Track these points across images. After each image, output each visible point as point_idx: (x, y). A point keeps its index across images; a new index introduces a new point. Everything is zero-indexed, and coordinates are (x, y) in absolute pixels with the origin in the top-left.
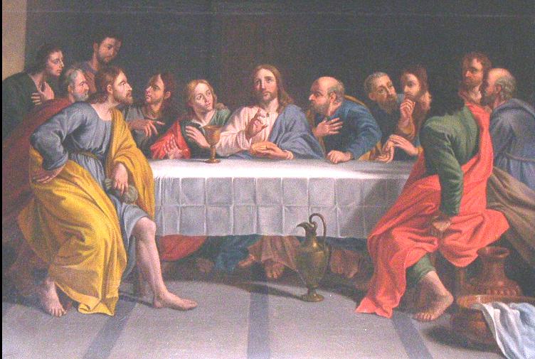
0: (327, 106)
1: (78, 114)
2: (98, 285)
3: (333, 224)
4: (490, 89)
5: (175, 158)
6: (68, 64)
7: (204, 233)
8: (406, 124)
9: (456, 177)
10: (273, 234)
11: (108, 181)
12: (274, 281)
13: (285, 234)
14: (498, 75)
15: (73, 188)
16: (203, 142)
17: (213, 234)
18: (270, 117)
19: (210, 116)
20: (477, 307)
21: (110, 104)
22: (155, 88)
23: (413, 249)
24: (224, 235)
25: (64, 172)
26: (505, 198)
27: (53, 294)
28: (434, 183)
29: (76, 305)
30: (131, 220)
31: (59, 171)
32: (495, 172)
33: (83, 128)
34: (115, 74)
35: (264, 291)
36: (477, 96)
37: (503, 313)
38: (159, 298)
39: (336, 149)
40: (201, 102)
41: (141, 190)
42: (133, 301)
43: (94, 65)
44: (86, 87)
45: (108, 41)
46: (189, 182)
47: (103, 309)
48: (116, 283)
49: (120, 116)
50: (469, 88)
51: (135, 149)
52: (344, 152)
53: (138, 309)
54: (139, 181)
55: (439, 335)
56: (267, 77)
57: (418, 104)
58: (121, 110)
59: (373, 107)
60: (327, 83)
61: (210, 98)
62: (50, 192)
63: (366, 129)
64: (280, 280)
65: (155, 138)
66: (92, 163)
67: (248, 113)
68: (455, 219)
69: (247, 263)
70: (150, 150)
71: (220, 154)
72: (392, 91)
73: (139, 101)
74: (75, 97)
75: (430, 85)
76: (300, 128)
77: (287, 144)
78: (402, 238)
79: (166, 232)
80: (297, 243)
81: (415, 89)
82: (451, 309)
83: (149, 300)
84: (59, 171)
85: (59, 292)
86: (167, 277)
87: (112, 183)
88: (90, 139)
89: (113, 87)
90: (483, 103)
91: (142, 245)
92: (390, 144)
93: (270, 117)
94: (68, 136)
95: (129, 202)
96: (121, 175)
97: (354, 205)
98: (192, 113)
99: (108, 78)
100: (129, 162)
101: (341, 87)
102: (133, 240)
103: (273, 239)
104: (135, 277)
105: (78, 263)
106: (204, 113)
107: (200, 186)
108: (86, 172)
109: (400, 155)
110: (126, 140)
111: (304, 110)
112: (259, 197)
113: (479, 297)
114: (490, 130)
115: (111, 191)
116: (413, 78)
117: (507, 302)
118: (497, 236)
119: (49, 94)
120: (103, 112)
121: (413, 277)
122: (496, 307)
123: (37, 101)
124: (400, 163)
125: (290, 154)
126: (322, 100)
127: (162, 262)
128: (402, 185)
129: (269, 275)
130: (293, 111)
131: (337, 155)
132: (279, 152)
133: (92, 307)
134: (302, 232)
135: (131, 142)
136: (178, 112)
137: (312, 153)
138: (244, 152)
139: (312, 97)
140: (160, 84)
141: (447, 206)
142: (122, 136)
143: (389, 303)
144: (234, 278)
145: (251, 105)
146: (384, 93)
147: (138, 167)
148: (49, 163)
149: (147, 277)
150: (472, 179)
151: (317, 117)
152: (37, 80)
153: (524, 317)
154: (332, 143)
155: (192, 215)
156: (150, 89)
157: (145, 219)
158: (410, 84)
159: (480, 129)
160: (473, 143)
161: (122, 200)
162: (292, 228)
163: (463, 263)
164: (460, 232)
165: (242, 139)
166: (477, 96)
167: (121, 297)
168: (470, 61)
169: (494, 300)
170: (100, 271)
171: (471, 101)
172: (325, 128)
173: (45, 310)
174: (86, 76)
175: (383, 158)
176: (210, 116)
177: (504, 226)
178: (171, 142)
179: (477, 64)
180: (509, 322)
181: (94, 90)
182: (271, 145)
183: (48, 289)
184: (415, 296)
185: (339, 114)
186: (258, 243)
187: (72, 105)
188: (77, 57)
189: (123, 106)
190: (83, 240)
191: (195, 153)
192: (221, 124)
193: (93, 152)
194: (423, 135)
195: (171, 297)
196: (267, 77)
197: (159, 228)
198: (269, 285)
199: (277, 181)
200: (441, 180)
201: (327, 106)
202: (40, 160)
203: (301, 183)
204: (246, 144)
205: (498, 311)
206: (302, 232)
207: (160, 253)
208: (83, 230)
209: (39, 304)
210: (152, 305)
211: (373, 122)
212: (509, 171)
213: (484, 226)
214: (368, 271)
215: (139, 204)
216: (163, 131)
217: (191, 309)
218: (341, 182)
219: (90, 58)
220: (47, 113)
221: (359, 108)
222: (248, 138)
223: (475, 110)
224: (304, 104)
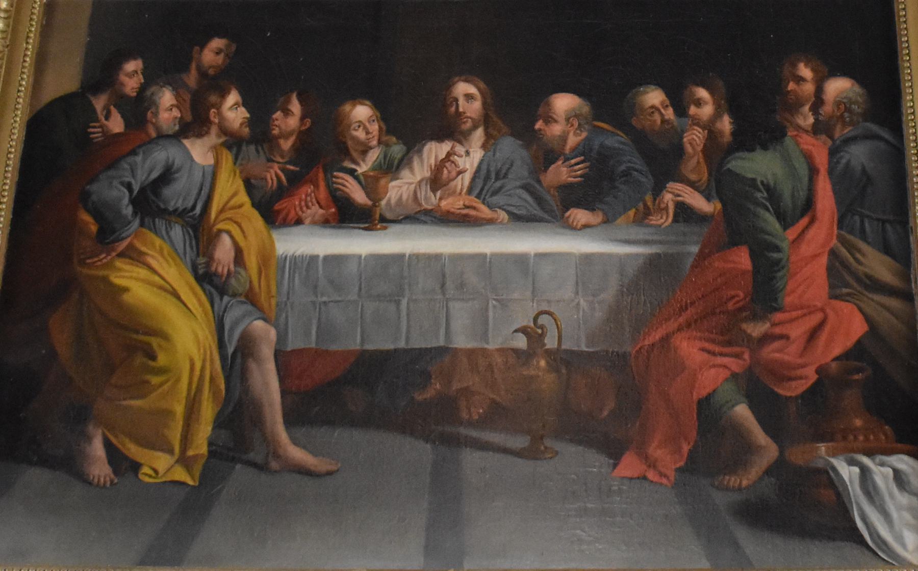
0: (564, 138)
1: (160, 156)
2: (175, 435)
4: (827, 109)
5: (314, 223)
6: (151, 77)
7: (355, 344)
8: (694, 163)
9: (778, 249)
10: (470, 345)
11: (202, 260)
12: (471, 424)
13: (491, 346)
15: (143, 272)
16: (359, 196)
17: (369, 347)
18: (470, 157)
19: (374, 155)
20: (820, 464)
21: (213, 138)
22: (287, 112)
24: (391, 347)
25: (131, 247)
26: (859, 280)
27: (98, 448)
29: (135, 467)
30: (235, 324)
31: (123, 245)
32: (843, 241)
33: (167, 176)
34: (224, 95)
35: (454, 442)
37: (865, 472)
38: (277, 456)
39: (578, 205)
40: (360, 134)
42: (233, 460)
43: (192, 79)
44: (176, 113)
45: (217, 43)
47: (180, 474)
48: (204, 430)
49: (227, 158)
50: (794, 106)
51: (248, 209)
52: (592, 210)
53: (241, 474)
54: (252, 261)
55: (760, 514)
56: (467, 95)
57: (712, 135)
58: (228, 146)
59: (641, 140)
60: (564, 103)
61: (375, 128)
62: (105, 280)
63: (626, 174)
64: (485, 422)
65: (282, 192)
66: (177, 232)
67: (435, 151)
68: (778, 316)
69: (429, 393)
70: (272, 210)
71: (389, 215)
72: (669, 113)
73: (260, 134)
74: (158, 129)
75: (732, 103)
76: (520, 172)
77: (495, 199)
78: (689, 349)
79: (293, 344)
80: (512, 360)
81: (707, 110)
82: (777, 468)
83: (259, 459)
84: (123, 245)
85: (109, 446)
86: (292, 419)
87: (208, 265)
88: (177, 195)
89: (219, 114)
90: (818, 129)
91: (252, 365)
92: (668, 197)
93: (470, 157)
94: (142, 190)
95: (234, 295)
96: (224, 252)
97: (609, 295)
98: (345, 152)
99: (213, 98)
100: (240, 228)
101: (586, 109)
102: (236, 358)
103: (471, 353)
104: (238, 417)
105: (142, 396)
106: (365, 150)
107: (353, 268)
108: (166, 248)
109: (684, 213)
110: (235, 194)
111: (527, 146)
112: (449, 284)
113: (822, 448)
114: (831, 172)
115: (206, 278)
116: (703, 93)
117: (870, 454)
118: (850, 343)
119: (116, 124)
120: (200, 151)
121: (709, 412)
122: (852, 462)
123: (96, 133)
124: (682, 227)
125: (503, 215)
126: (557, 129)
127: (284, 393)
128: (690, 261)
129: (464, 415)
130: (509, 147)
131: (580, 215)
132: (485, 212)
133: (161, 470)
134: (521, 342)
135: (243, 197)
136: (323, 149)
137: (538, 212)
138: (427, 212)
139: (539, 125)
140: (296, 107)
141: (765, 291)
142: (229, 188)
143: (669, 461)
145: (440, 138)
146: (657, 117)
147: (252, 239)
148: (108, 234)
150: (806, 249)
151: (548, 156)
152: (99, 103)
153: (899, 478)
156: (278, 114)
157: (259, 324)
158: (699, 103)
159: (813, 171)
160: (802, 194)
161: (222, 292)
162: (506, 336)
163: (796, 389)
164: (786, 337)
165: (425, 193)
167: (212, 454)
168: (794, 66)
169: (849, 453)
170: (179, 409)
171: (799, 128)
172: (561, 173)
173: (86, 481)
174: (177, 96)
175: (655, 220)
176: (374, 155)
177: (859, 328)
178: (310, 199)
179: (805, 72)
180: (875, 487)
181: (189, 118)
182: (473, 200)
183: (89, 439)
184: (712, 446)
185: (583, 150)
186: (447, 359)
187: (151, 141)
188: (167, 66)
189: (233, 142)
190: (153, 357)
191: (347, 215)
192: (390, 168)
193: (181, 214)
194: (721, 183)
195: (297, 454)
196: (467, 95)
197: (282, 337)
198: (463, 431)
200: (753, 256)
201: (564, 138)
202: (94, 228)
203: (521, 260)
204: (430, 200)
205: (856, 470)
206: (521, 342)
207: (282, 380)
208: (154, 342)
209: (70, 465)
210: (261, 467)
211: (638, 163)
212: (864, 238)
213: (827, 328)
215: (251, 298)
216: (295, 180)
217: (329, 473)
218: (587, 259)
219: (186, 68)
220: (114, 152)
221: (616, 140)
222: (434, 190)
223: (806, 142)
224: (526, 134)
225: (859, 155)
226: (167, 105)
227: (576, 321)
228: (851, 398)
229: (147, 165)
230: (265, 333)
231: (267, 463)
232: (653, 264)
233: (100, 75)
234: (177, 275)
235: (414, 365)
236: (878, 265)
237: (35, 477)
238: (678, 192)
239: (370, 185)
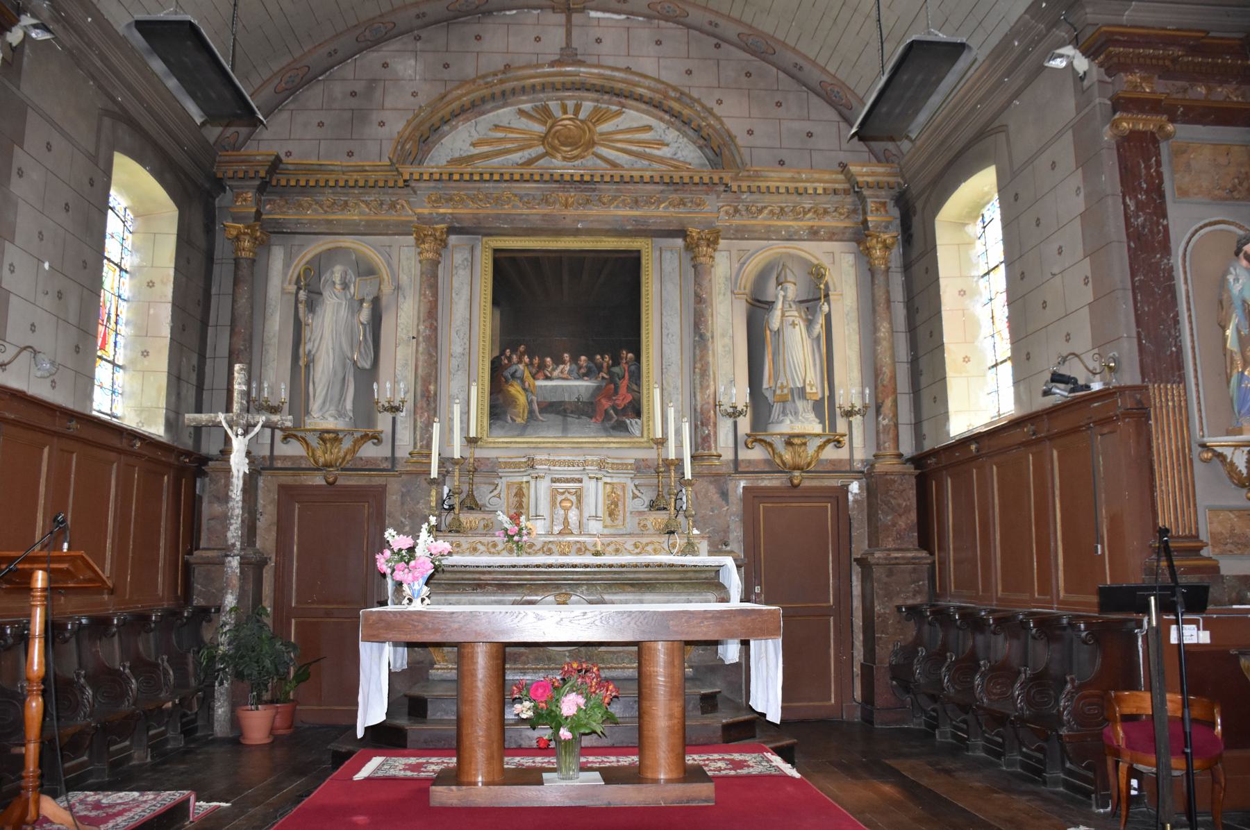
1: (514, 368)
3: (585, 397)
6: (512, 352)
8: (605, 369)
14: (630, 355)
18: (567, 368)
23: (606, 404)
28: (612, 386)
55: (614, 428)
60: (583, 358)
70: (534, 377)
73: (531, 364)
75: (612, 358)
78: (604, 401)
88: (518, 374)
93: (567, 368)
100: (529, 380)
102: (530, 403)
104: (531, 412)
115: (524, 389)
120: (521, 366)
130: (574, 366)
136: (542, 366)
141: (616, 392)
142: (527, 373)
144: (558, 413)
148: (507, 381)
151: (580, 368)
162: (574, 399)
172: (583, 371)
178: (540, 375)
184: (607, 417)
188: (514, 351)
189: (527, 365)
191: (547, 378)
192: (554, 370)
194: (609, 372)
214: (594, 411)
224: (577, 364)
225: (633, 368)
230: (534, 398)
231: (537, 420)
233: (502, 353)
234: (519, 388)
235: (561, 403)
236: (635, 387)
237: (500, 423)
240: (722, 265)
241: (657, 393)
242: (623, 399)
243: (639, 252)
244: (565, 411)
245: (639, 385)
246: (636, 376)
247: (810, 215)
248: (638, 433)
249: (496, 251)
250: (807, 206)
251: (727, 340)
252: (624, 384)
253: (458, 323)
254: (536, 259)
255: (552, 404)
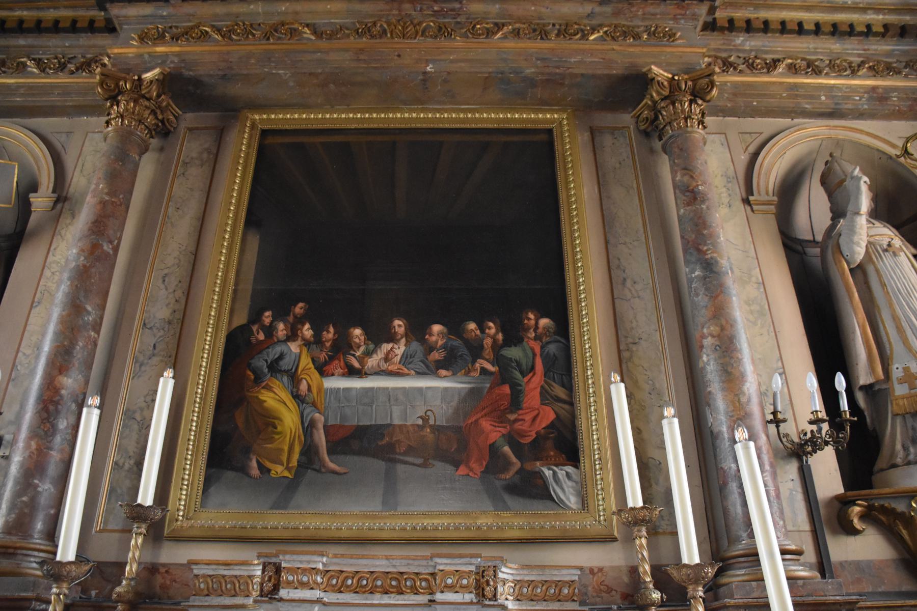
0: (437, 342)
1: (278, 349)
2: (284, 459)
4: (540, 331)
5: (339, 375)
6: (275, 318)
7: (355, 423)
8: (488, 352)
9: (520, 385)
10: (400, 423)
11: (295, 390)
12: (400, 454)
13: (408, 423)
14: (544, 322)
15: (272, 395)
16: (356, 365)
17: (361, 424)
18: (400, 349)
19: (362, 349)
20: (537, 470)
21: (299, 342)
22: (328, 332)
24: (369, 423)
25: (267, 384)
26: (552, 397)
27: (254, 464)
29: (269, 471)
31: (264, 384)
32: (546, 382)
33: (281, 357)
34: (303, 325)
35: (394, 461)
36: (532, 334)
37: (555, 473)
38: (324, 466)
39: (442, 368)
40: (357, 340)
41: (315, 395)
42: (307, 468)
43: (291, 319)
44: (285, 332)
45: (301, 305)
46: (347, 390)
48: (296, 456)
49: (305, 350)
50: (527, 330)
51: (313, 369)
54: (314, 390)
56: (399, 325)
58: (305, 345)
59: (467, 343)
60: (437, 328)
61: (362, 338)
62: (257, 397)
63: (461, 356)
64: (406, 453)
65: (326, 363)
66: (285, 379)
67: (386, 347)
68: (521, 412)
69: (384, 442)
70: (323, 370)
72: (478, 332)
73: (318, 340)
74: (278, 338)
75: (503, 328)
76: (420, 355)
77: (410, 366)
78: (486, 424)
79: (331, 423)
80: (416, 429)
81: (493, 331)
82: (521, 471)
83: (317, 467)
84: (264, 384)
85: (258, 462)
86: (330, 452)
87: (297, 392)
88: (285, 364)
89: (302, 332)
90: (537, 338)
91: (315, 431)
92: (477, 365)
93: (400, 349)
94: (272, 362)
96: (303, 386)
97: (454, 403)
98: (351, 348)
99: (299, 326)
100: (310, 377)
101: (445, 330)
102: (308, 428)
103: (400, 426)
104: (309, 452)
106: (359, 347)
107: (354, 393)
109: (484, 371)
111: (422, 345)
113: (538, 463)
114: (541, 355)
115: (297, 397)
116: (491, 324)
117: (557, 466)
118: (549, 422)
119: (261, 337)
120: (294, 347)
121: (493, 449)
122: (549, 469)
123: (253, 340)
124: (483, 377)
125: (413, 372)
126: (434, 338)
127: (327, 442)
130: (415, 345)
131: (443, 372)
132: (406, 371)
134: (420, 422)
135: (311, 365)
136: (342, 346)
137: (427, 371)
138: (383, 371)
139: (427, 337)
140: (332, 330)
141: (516, 402)
142: (306, 361)
143: (478, 468)
145: (388, 342)
146: (473, 334)
147: (315, 382)
148: (258, 379)
149: (317, 452)
150: (531, 386)
151: (431, 349)
152: (255, 328)
153: (568, 475)
154: (441, 365)
155: (348, 411)
156: (325, 333)
157: (317, 415)
158: (490, 328)
159: (534, 355)
160: (530, 364)
161: (303, 402)
162: (414, 419)
163: (527, 440)
164: (523, 420)
165: (382, 363)
166: (532, 334)
168: (527, 313)
170: (286, 448)
171: (529, 338)
172: (436, 356)
173: (248, 475)
174: (285, 325)
175: (473, 374)
176: (362, 349)
177: (552, 416)
179: (531, 316)
181: (290, 334)
182: (401, 366)
183: (251, 460)
184: (495, 462)
185: (444, 347)
186: (391, 428)
187: (275, 343)
188: (281, 313)
189: (307, 344)
190: (276, 428)
191: (352, 372)
192: (369, 354)
193: (287, 372)
194: (498, 360)
195: (332, 466)
196: (399, 325)
197: (326, 420)
198: (397, 457)
199: (404, 389)
200: (511, 388)
201: (437, 342)
202: (253, 377)
203: (420, 390)
204: (384, 366)
206: (420, 422)
207: (326, 437)
208: (276, 422)
209: (243, 470)
210: (318, 471)
211: (466, 351)
212: (554, 381)
213: (540, 416)
215: (314, 404)
216: (331, 358)
217: (345, 473)
218: (446, 389)
219: (289, 315)
220: (261, 347)
221: (457, 343)
224: (422, 340)
225: (552, 348)
226: (281, 329)
227: (442, 414)
228: (549, 444)
229: (273, 353)
231: (321, 469)
232: (471, 392)
233: (255, 317)
234: (285, 396)
235: (378, 431)
236: (560, 392)
237: (230, 475)
238: (481, 363)
239: (361, 360)
240: (716, 157)
241: (619, 393)
242: (535, 416)
243: (550, 132)
244: (391, 447)
245: (569, 387)
246: (562, 367)
247: (863, 71)
248: (572, 501)
249: (264, 133)
250: (857, 60)
251: (752, 291)
252: (533, 385)
253: (170, 261)
254: (343, 146)
255: (361, 432)
